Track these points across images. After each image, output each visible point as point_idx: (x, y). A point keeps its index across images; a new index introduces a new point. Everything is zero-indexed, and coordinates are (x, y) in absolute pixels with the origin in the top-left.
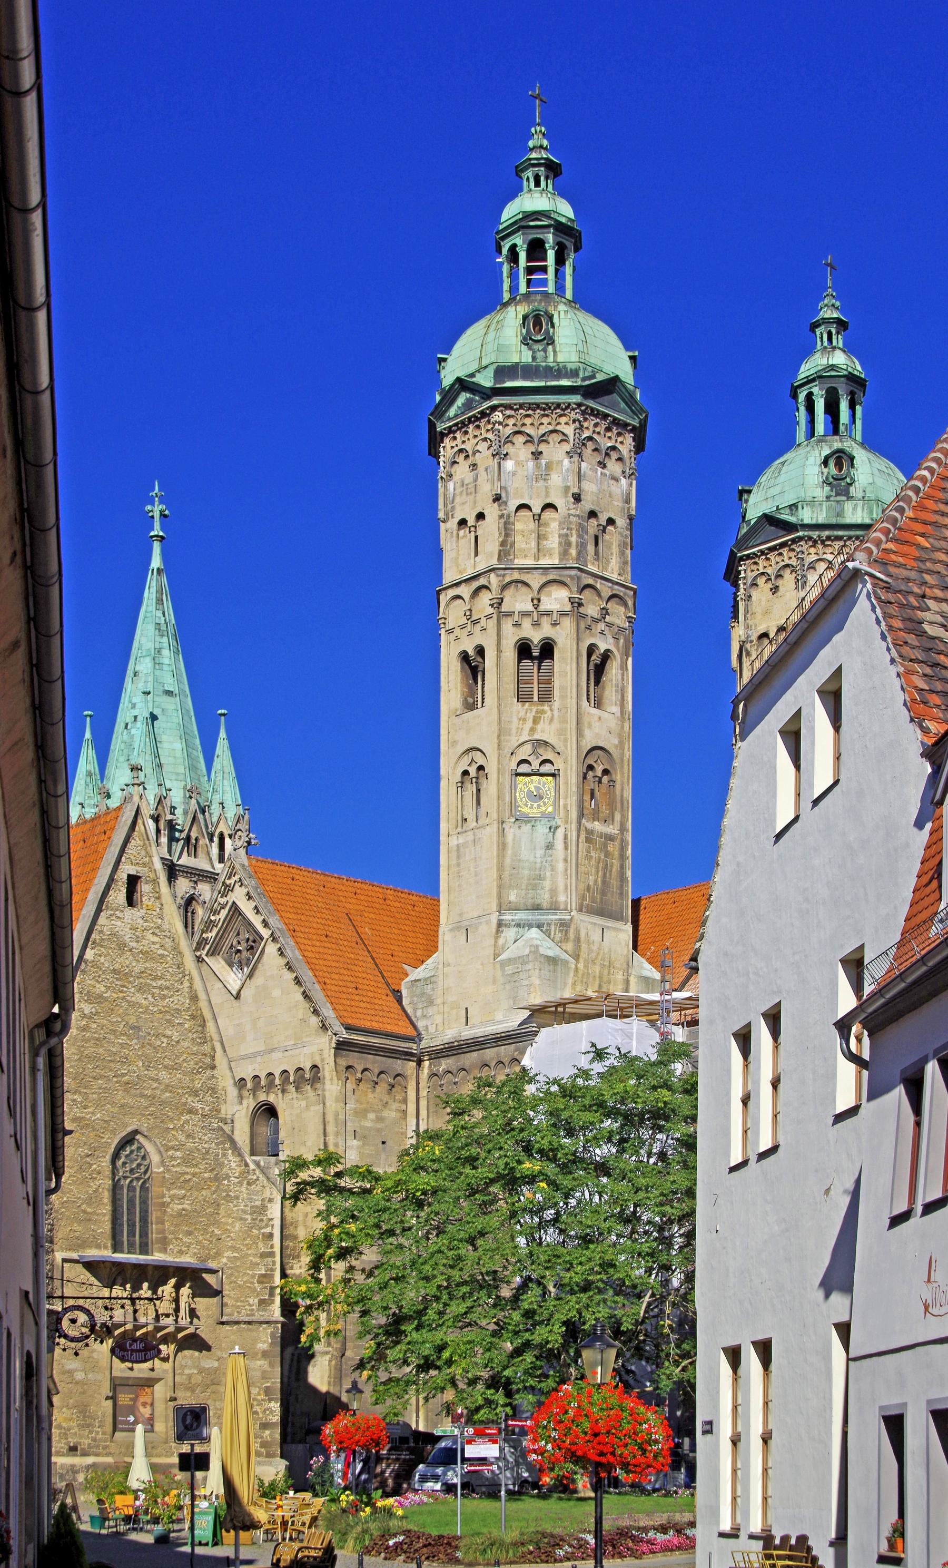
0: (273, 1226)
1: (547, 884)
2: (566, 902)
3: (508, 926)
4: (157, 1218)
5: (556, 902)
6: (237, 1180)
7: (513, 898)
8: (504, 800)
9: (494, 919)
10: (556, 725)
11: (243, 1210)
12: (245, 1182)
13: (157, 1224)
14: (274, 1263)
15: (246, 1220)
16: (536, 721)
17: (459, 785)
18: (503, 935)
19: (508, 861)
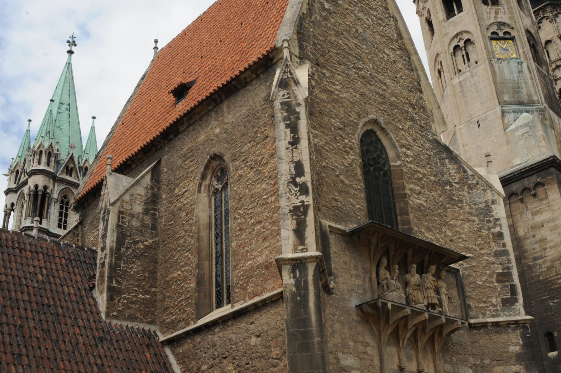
0: (500, 225)
1: (524, 91)
2: (538, 100)
3: (509, 112)
4: (400, 208)
5: (532, 100)
6: (457, 186)
7: (506, 98)
8: (488, 50)
9: (498, 109)
10: (507, 15)
11: (469, 213)
12: (466, 187)
13: (401, 215)
14: (509, 262)
15: (474, 221)
16: (496, 13)
17: (452, 54)
18: (506, 117)
19: (498, 80)
